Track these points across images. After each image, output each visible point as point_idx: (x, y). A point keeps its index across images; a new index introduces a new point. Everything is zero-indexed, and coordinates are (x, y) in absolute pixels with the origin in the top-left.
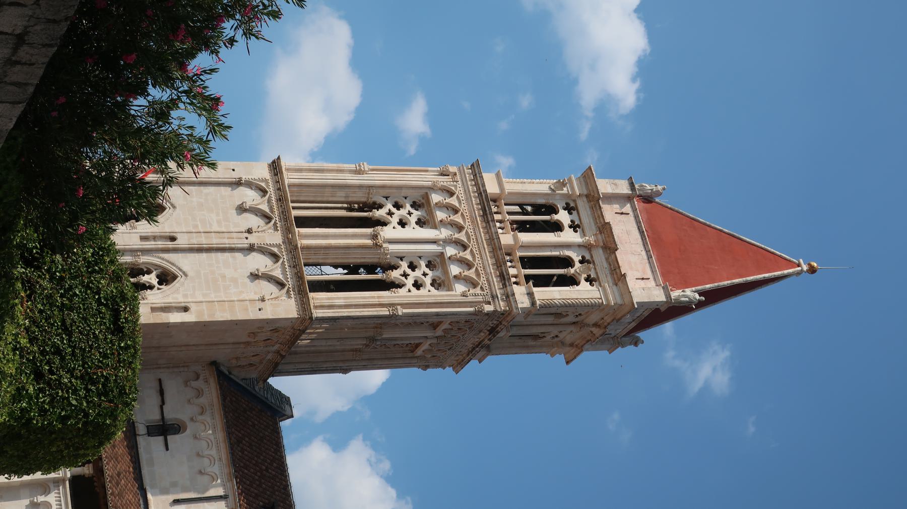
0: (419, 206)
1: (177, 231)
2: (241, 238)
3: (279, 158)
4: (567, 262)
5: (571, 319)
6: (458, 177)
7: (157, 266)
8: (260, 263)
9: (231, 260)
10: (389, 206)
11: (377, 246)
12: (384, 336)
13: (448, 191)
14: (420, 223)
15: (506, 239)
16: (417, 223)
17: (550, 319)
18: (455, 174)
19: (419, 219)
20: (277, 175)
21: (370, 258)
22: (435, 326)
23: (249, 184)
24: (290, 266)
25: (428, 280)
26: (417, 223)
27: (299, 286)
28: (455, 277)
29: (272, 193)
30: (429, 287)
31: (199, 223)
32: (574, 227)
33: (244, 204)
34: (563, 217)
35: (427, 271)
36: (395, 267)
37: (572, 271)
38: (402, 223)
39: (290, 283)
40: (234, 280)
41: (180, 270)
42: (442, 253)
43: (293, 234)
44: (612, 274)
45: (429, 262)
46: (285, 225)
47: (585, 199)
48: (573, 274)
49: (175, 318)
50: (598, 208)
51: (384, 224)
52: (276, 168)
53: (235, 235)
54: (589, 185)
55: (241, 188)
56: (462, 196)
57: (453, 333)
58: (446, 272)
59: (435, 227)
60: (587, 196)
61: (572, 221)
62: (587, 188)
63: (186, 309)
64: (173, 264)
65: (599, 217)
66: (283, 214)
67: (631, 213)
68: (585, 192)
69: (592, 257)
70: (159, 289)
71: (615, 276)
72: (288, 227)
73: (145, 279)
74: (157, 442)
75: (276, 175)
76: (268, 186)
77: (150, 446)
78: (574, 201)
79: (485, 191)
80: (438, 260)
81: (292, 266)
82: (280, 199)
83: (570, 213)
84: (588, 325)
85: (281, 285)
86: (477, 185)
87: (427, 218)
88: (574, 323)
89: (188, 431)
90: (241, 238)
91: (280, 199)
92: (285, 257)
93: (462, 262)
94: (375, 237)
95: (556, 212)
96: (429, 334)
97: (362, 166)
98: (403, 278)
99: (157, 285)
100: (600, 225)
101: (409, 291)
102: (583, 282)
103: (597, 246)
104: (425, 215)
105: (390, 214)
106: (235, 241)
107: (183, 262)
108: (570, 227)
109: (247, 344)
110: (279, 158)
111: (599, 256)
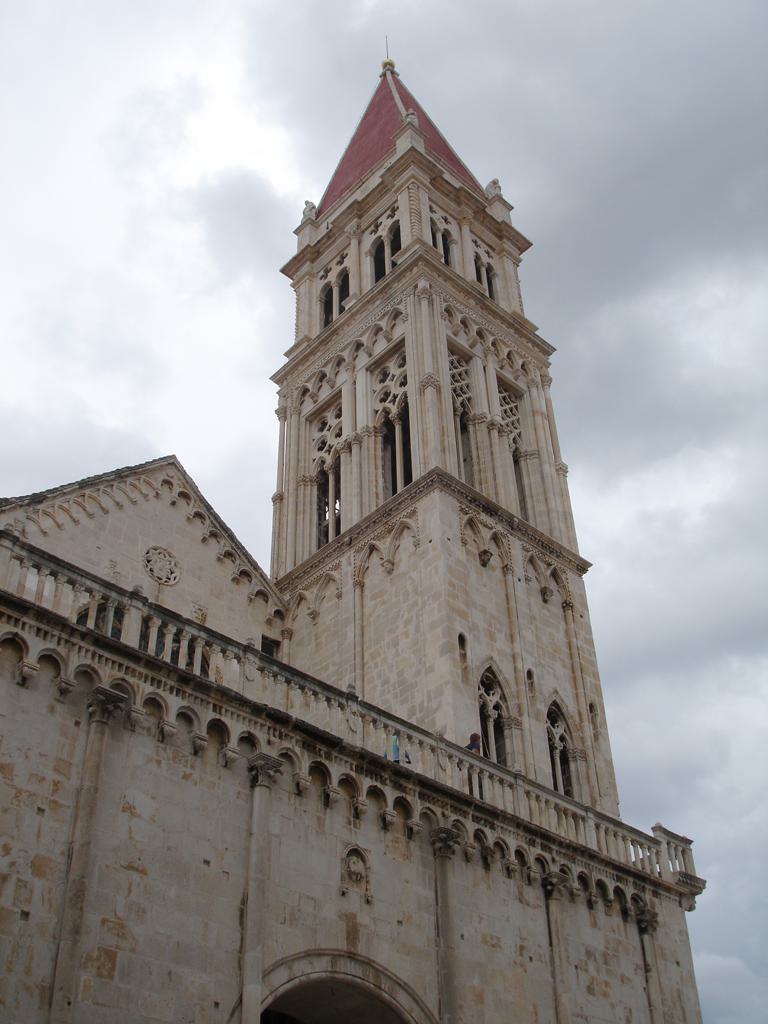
11: (358, 439)
12: (486, 410)
21: (373, 446)
42: (367, 370)
96: (477, 365)
98: (397, 400)
102: (395, 219)
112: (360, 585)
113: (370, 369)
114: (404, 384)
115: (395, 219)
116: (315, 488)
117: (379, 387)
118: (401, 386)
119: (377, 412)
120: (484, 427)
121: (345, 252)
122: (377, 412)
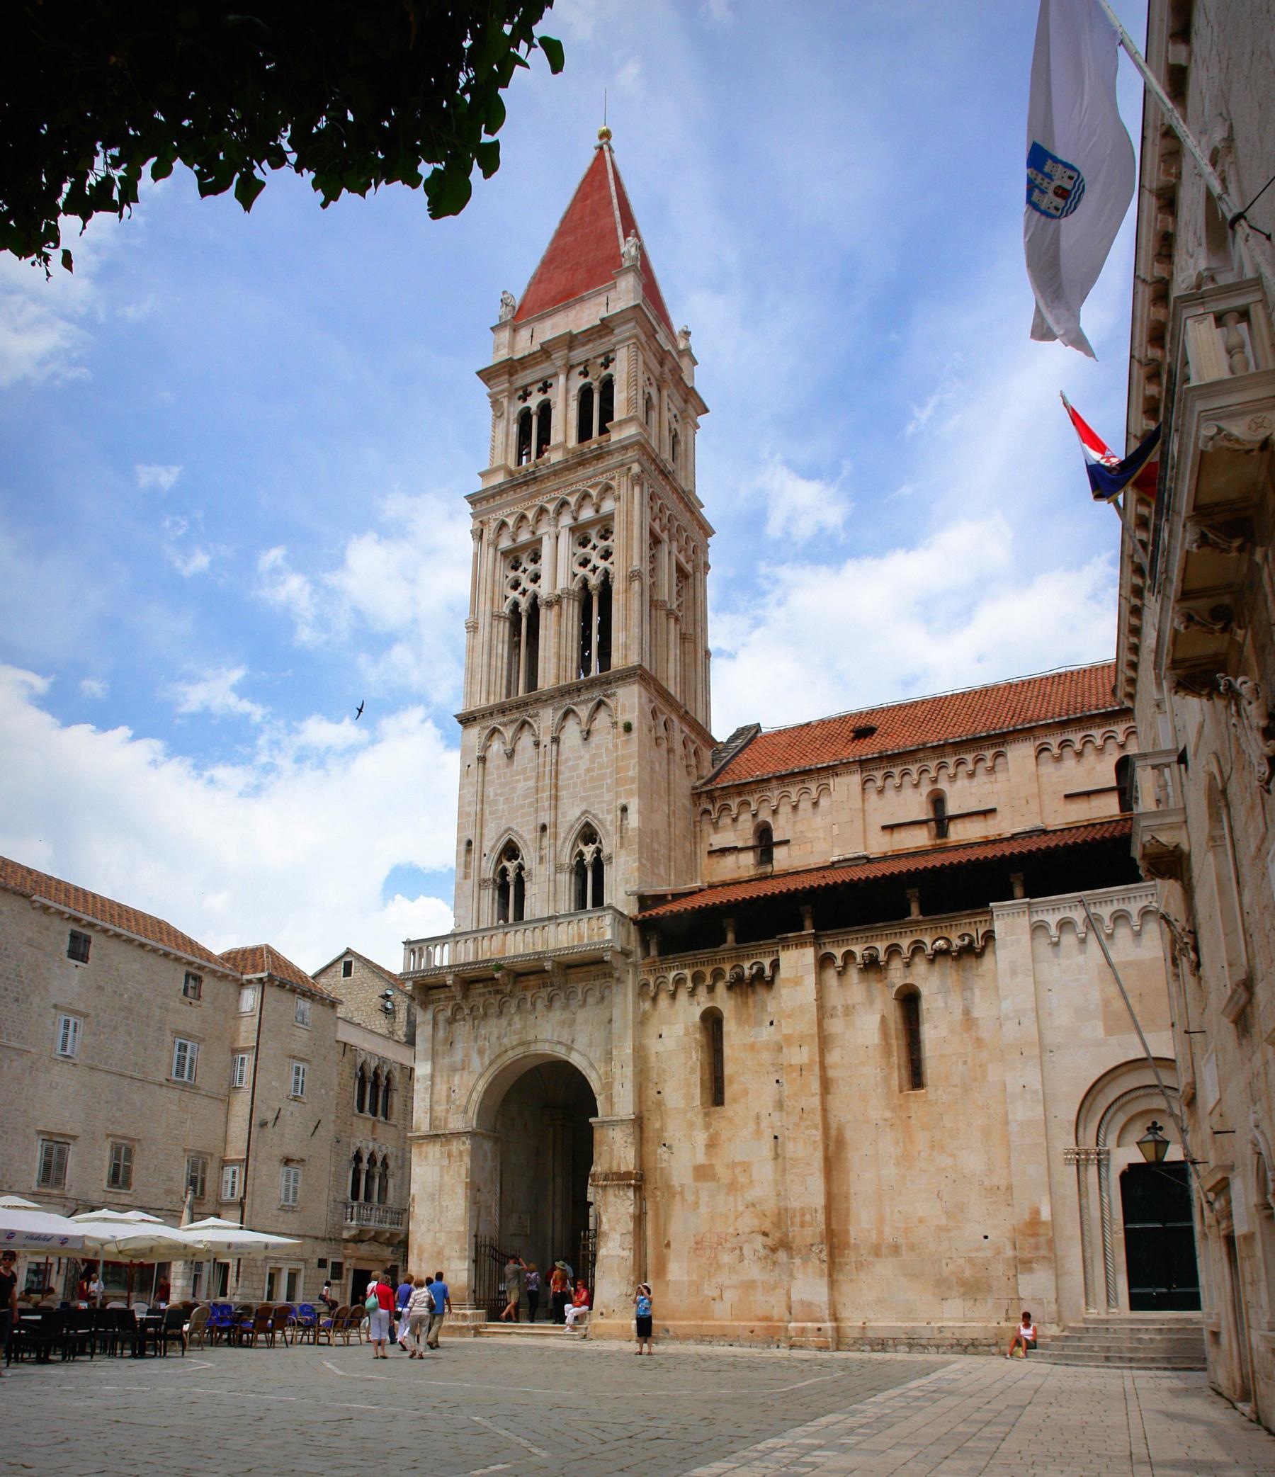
0: (517, 561)
1: (534, 824)
3: (456, 716)
4: (586, 393)
5: (653, 391)
6: (484, 518)
7: (575, 845)
8: (572, 732)
9: (570, 764)
11: (558, 600)
13: (500, 529)
14: (536, 558)
15: (555, 457)
16: (536, 562)
17: (654, 415)
18: (481, 522)
19: (531, 561)
21: (572, 611)
22: (655, 541)
23: (486, 748)
25: (602, 544)
26: (536, 562)
27: (602, 684)
28: (597, 511)
30: (608, 542)
32: (545, 388)
34: (533, 403)
35: (590, 546)
36: (585, 581)
37: (596, 385)
38: (536, 578)
39: (597, 694)
40: (593, 759)
41: (579, 818)
42: (570, 529)
43: (542, 693)
45: (580, 544)
47: (515, 377)
48: (600, 382)
49: (633, 820)
51: (535, 597)
53: (541, 760)
55: (489, 755)
56: (507, 511)
57: (665, 520)
58: (591, 523)
59: (540, 541)
60: (511, 375)
61: (539, 390)
62: (501, 375)
63: (624, 809)
64: (572, 827)
65: (534, 359)
67: (532, 325)
68: (506, 377)
69: (579, 364)
70: (600, 842)
73: (588, 858)
74: (779, 853)
75: (475, 719)
76: (488, 727)
77: (782, 859)
78: (517, 390)
79: (500, 485)
80: (578, 534)
83: (531, 393)
84: (662, 373)
85: (600, 704)
86: (493, 496)
87: (530, 551)
88: (659, 390)
89: (769, 820)
92: (568, 703)
93: (580, 507)
94: (549, 605)
95: (529, 409)
96: (665, 548)
98: (598, 571)
99: (597, 845)
100: (544, 357)
101: (612, 563)
103: (568, 359)
104: (526, 554)
105: (524, 592)
106: (548, 759)
107: (571, 814)
108: (545, 392)
109: (670, 751)
110: (456, 716)
111: (579, 355)
112: (556, 740)
113: (572, 530)
114: (606, 555)
115: (608, 371)
116: (507, 625)
117: (581, 551)
118: (602, 557)
119: (575, 575)
120: (663, 613)
121: (549, 382)
122: (575, 575)
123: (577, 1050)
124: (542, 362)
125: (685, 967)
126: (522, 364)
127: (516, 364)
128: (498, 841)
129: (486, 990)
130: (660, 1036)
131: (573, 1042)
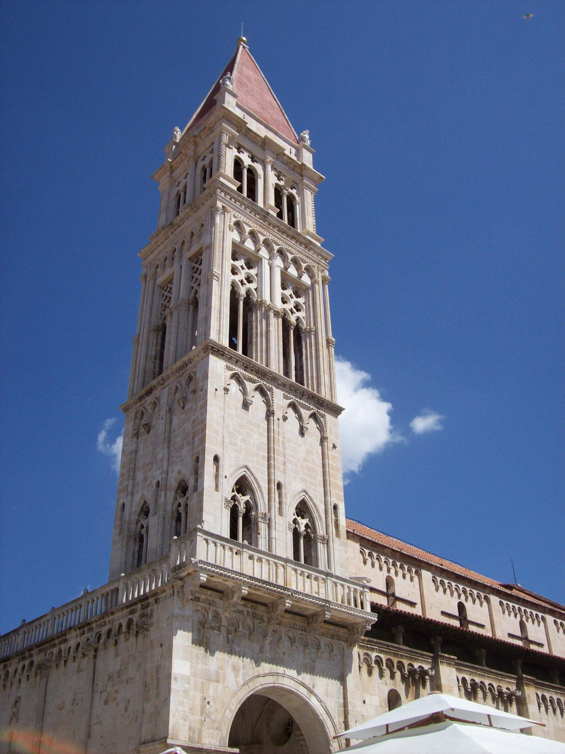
2: (279, 424)
6: (228, 208)
10: (237, 278)
18: (223, 207)
20: (225, 353)
24: (301, 399)
29: (239, 370)
31: (261, 453)
33: (249, 401)
44: (293, 170)
46: (268, 378)
50: (250, 132)
52: (219, 351)
54: (233, 121)
64: (295, 496)
66: (258, 374)
71: (296, 169)
72: (271, 377)
81: (301, 397)
82: (245, 367)
90: (279, 424)
91: (245, 367)
97: (217, 274)
100: (260, 143)
112: (285, 419)
121: (255, 159)
123: (316, 696)
124: (256, 144)
125: (381, 651)
126: (246, 132)
127: (244, 130)
128: (236, 471)
129: (245, 610)
130: (364, 702)
131: (314, 687)
